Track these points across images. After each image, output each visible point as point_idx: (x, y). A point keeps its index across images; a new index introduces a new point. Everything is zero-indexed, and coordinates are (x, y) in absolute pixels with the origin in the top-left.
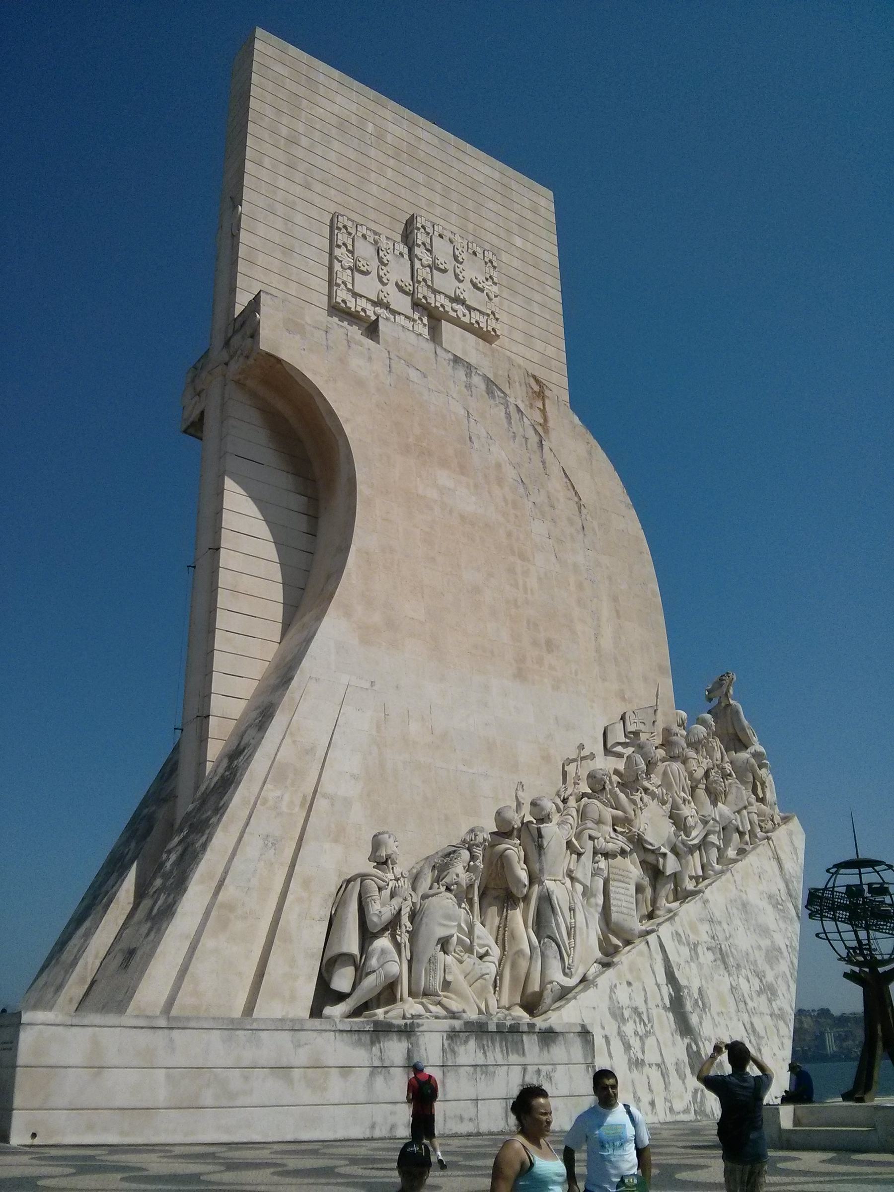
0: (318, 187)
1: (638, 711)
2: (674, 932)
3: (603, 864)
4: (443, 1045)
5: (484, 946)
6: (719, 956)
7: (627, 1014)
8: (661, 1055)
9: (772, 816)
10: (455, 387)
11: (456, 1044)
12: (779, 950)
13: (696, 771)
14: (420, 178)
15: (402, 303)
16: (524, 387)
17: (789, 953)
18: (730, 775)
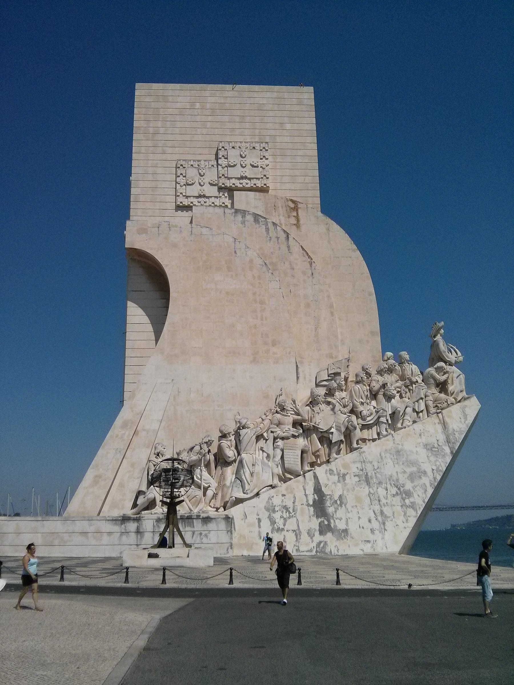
0: (169, 150)
1: (336, 363)
2: (328, 470)
3: (280, 443)
4: (154, 524)
5: (208, 483)
6: (364, 478)
7: (277, 509)
8: (298, 526)
9: (447, 400)
10: (235, 225)
11: (160, 523)
13: (374, 386)
14: (226, 119)
15: (213, 191)
16: (285, 209)
17: (434, 474)
18: (417, 382)
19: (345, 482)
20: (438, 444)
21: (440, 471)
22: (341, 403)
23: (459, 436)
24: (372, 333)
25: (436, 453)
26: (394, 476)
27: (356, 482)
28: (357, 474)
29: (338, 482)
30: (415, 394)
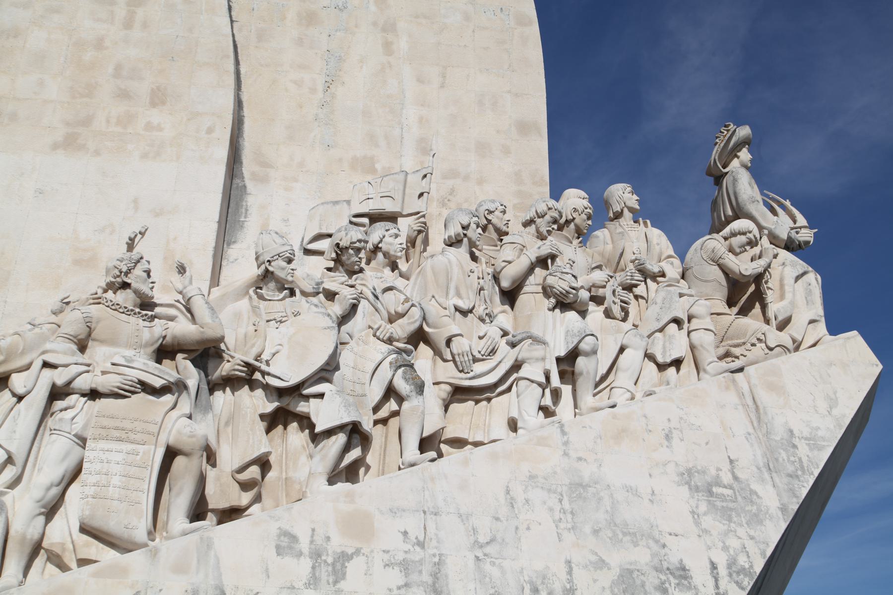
6: (426, 578)
12: (682, 573)
13: (510, 262)
17: (716, 580)
18: (663, 275)
19: (342, 585)
20: (733, 474)
21: (742, 571)
22: (379, 306)
23: (810, 454)
24: (523, 128)
25: (724, 504)
26: (554, 575)
27: (390, 590)
28: (400, 557)
29: (308, 585)
30: (653, 310)
